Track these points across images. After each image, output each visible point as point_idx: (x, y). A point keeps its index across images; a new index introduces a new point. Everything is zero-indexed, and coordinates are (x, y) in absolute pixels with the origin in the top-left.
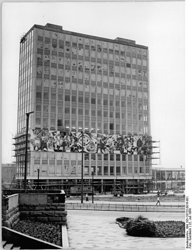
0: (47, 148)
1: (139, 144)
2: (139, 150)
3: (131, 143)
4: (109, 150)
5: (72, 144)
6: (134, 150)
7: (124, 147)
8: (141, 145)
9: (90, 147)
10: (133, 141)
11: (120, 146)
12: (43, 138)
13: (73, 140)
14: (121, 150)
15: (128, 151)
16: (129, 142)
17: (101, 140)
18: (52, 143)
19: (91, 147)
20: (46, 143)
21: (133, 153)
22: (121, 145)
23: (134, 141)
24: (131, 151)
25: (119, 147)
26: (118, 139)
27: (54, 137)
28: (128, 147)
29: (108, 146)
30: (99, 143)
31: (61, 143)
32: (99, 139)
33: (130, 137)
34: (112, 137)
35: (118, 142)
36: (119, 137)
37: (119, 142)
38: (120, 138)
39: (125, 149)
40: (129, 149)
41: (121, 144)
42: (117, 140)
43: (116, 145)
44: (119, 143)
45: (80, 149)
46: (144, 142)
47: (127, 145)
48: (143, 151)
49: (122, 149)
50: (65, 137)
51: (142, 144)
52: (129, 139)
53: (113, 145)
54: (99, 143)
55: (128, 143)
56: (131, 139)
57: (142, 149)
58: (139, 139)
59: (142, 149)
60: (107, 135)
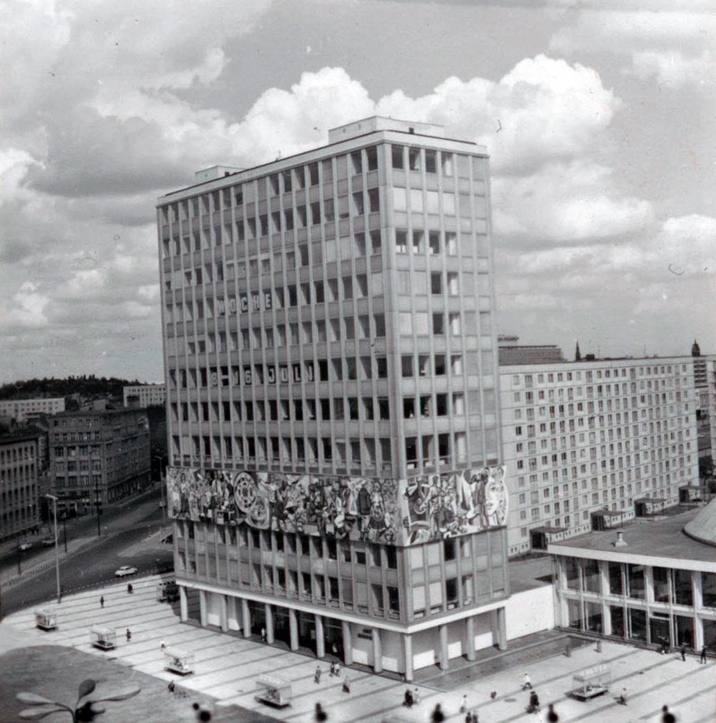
0: (189, 512)
1: (363, 506)
2: (363, 525)
3: (343, 501)
4: (294, 523)
5: (226, 503)
6: (350, 525)
7: (326, 515)
9: (256, 513)
10: (347, 496)
11: (317, 511)
12: (183, 486)
14: (319, 524)
15: (336, 529)
16: (338, 499)
17: (276, 492)
18: (196, 500)
19: (259, 513)
20: (187, 501)
21: (348, 536)
22: (320, 507)
23: (349, 495)
24: (344, 527)
25: (314, 514)
26: (313, 488)
27: (198, 483)
29: (291, 510)
30: (273, 500)
31: (209, 500)
32: (273, 487)
33: (339, 482)
34: (298, 484)
35: (312, 498)
36: (315, 480)
37: (315, 498)
38: (316, 483)
39: (328, 521)
40: (339, 520)
41: (318, 503)
42: (312, 491)
43: (308, 507)
44: (313, 502)
45: (240, 517)
46: (376, 498)
47: (333, 509)
48: (376, 530)
49: (322, 520)
50: (214, 482)
51: (372, 504)
52: (336, 486)
53: (301, 509)
54: (273, 500)
55: (335, 500)
57: (373, 523)
58: (363, 490)
59: (373, 523)
60: (289, 476)
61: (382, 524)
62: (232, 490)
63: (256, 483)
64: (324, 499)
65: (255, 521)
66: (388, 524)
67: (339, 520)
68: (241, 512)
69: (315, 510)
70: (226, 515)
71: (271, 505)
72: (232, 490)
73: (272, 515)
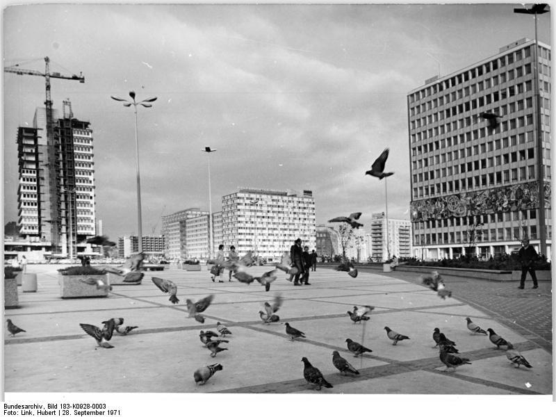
1: (519, 195)
7: (498, 203)
8: (521, 197)
12: (419, 208)
13: (444, 205)
15: (503, 208)
21: (510, 209)
22: (495, 201)
28: (503, 202)
30: (468, 203)
32: (469, 198)
40: (505, 205)
46: (526, 191)
51: (523, 194)
52: (504, 191)
54: (468, 203)
56: (507, 190)
57: (523, 202)
58: (519, 189)
59: (523, 202)
61: (530, 200)
62: (446, 204)
63: (459, 198)
64: (497, 198)
65: (458, 214)
66: (532, 200)
67: (505, 205)
68: (450, 212)
69: (491, 203)
70: (442, 215)
71: (468, 206)
72: (446, 204)
73: (468, 210)
